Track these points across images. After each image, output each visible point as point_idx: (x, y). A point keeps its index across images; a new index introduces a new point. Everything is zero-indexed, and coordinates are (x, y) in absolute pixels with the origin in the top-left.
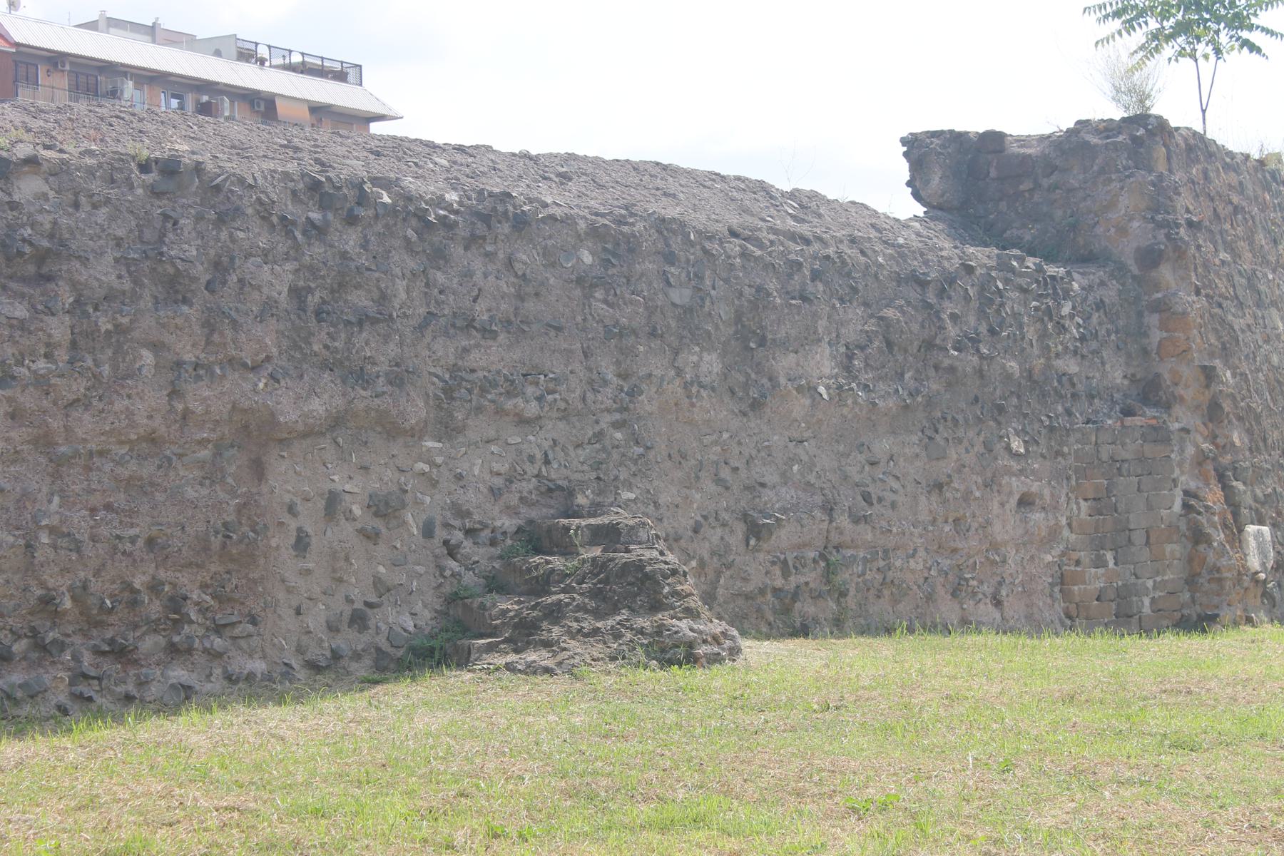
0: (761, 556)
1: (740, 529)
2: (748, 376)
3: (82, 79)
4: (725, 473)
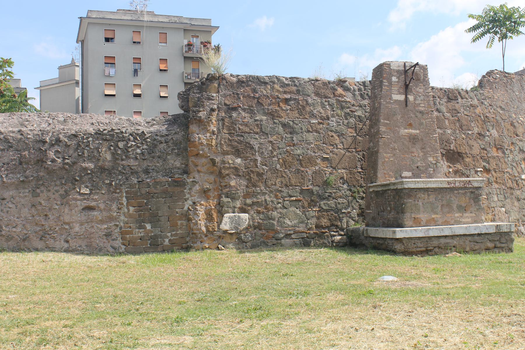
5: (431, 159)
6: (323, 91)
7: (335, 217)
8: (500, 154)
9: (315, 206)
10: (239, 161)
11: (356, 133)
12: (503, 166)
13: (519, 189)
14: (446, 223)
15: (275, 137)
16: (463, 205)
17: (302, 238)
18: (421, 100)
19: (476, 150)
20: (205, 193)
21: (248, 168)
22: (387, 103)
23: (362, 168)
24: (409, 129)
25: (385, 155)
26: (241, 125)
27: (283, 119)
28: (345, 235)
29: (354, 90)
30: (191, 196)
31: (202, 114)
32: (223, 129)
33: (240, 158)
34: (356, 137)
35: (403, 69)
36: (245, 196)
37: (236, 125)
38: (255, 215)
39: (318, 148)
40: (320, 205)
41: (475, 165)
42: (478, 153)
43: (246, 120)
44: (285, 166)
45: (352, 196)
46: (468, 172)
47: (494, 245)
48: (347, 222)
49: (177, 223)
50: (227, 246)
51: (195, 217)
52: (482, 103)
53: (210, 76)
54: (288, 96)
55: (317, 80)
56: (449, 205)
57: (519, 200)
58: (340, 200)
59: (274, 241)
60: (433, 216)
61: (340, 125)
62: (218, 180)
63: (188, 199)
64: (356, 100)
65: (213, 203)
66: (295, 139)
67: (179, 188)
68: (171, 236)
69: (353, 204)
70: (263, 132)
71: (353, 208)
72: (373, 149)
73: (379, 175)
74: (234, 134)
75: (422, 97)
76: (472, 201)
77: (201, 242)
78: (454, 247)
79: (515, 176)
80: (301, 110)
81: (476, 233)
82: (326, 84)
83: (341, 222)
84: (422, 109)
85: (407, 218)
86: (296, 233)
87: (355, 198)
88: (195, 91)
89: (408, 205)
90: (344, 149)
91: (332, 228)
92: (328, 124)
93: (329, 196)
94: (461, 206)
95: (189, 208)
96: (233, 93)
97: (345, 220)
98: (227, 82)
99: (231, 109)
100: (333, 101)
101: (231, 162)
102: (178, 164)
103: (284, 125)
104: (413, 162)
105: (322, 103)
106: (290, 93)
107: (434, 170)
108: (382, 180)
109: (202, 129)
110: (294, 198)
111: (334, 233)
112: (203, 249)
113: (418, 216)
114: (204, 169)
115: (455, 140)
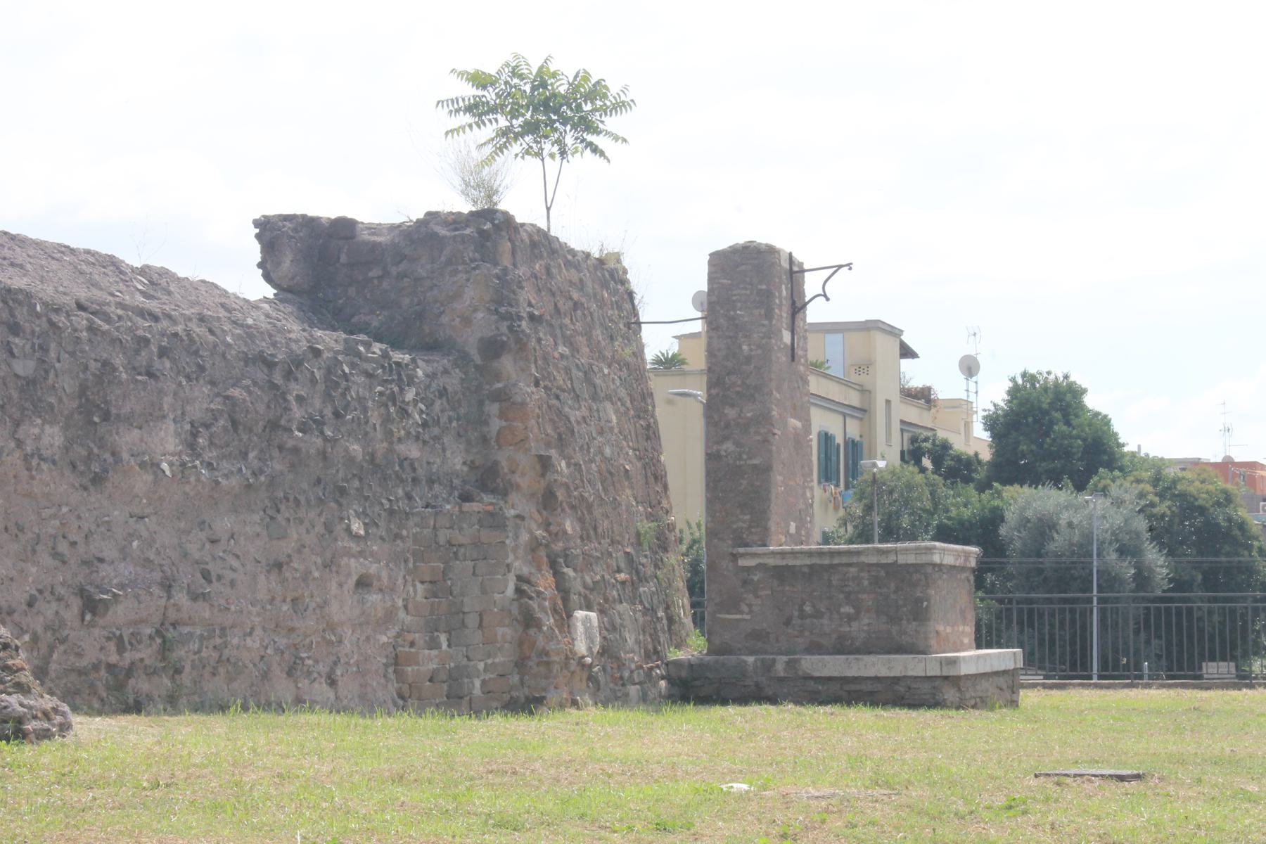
0: (96, 632)
1: (76, 603)
2: (90, 452)
4: (63, 547)
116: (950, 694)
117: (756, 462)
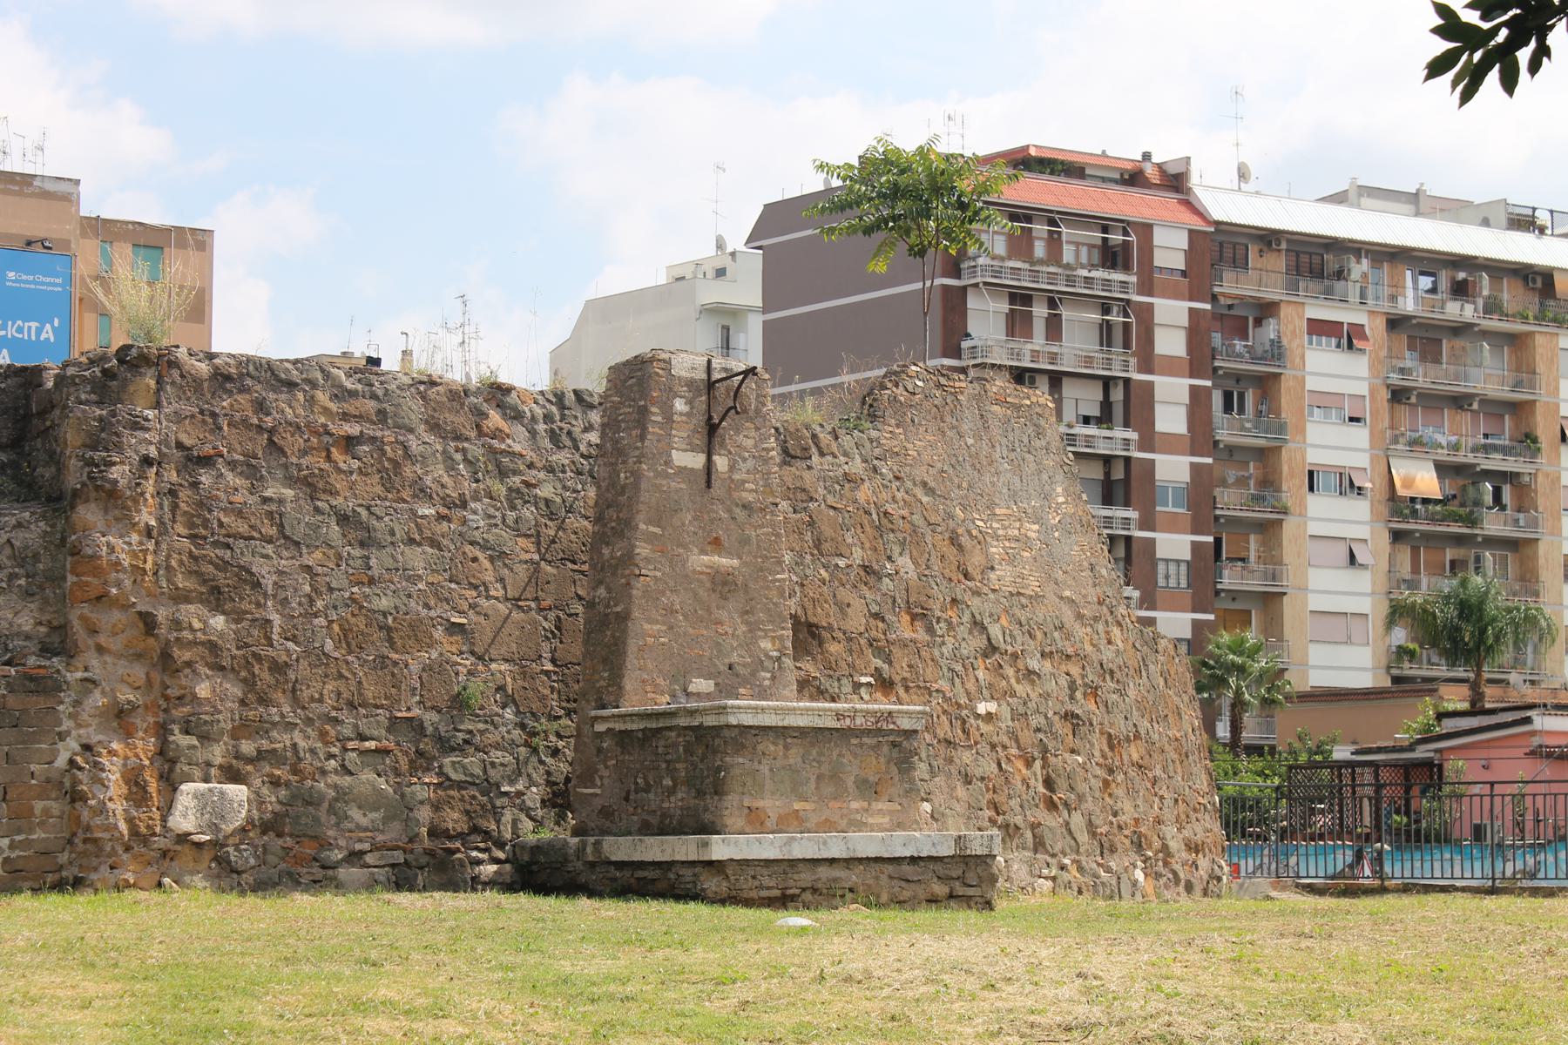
3: (1305, 259)
5: (766, 644)
6: (450, 417)
7: (483, 806)
8: (922, 635)
9: (428, 770)
10: (219, 622)
11: (539, 551)
12: (929, 671)
13: (970, 747)
14: (828, 826)
15: (318, 555)
16: (871, 778)
17: (393, 866)
18: (748, 472)
19: (856, 620)
20: (120, 716)
21: (247, 645)
22: (658, 475)
23: (553, 661)
24: (713, 553)
25: (647, 626)
26: (224, 510)
27: (340, 500)
28: (506, 861)
29: (533, 419)
30: (79, 726)
31: (119, 473)
32: (174, 521)
33: (224, 613)
34: (538, 563)
35: (704, 376)
36: (236, 735)
37: (210, 511)
38: (265, 791)
39: (436, 594)
40: (440, 767)
41: (852, 666)
42: (862, 629)
43: (238, 498)
44: (348, 645)
45: (527, 744)
46: (833, 687)
47: (947, 890)
48: (515, 822)
49: (32, 808)
50: (187, 879)
51: (97, 788)
52: (875, 470)
53: (134, 352)
54: (353, 429)
55: (433, 383)
56: (836, 777)
57: (968, 780)
58: (497, 756)
59: (319, 873)
60: (797, 806)
61: (496, 525)
62: (156, 677)
63: (68, 733)
64: (537, 449)
65: (145, 746)
66: (373, 562)
67: (41, 699)
68: (12, 847)
69: (531, 770)
70: (286, 538)
71: (532, 783)
72: (608, 606)
73: (629, 684)
74: (205, 538)
75: (750, 463)
76: (894, 770)
77: (112, 868)
78: (851, 890)
79: (959, 706)
80: (390, 474)
81: (908, 853)
82: (458, 395)
83: (498, 822)
84: (750, 497)
85: (732, 808)
86: (378, 849)
87: (535, 750)
88: (83, 397)
89: (736, 771)
90: (507, 599)
91: (472, 837)
92: (464, 522)
93: (465, 741)
94: (866, 781)
95: (72, 762)
96: (202, 412)
97: (508, 817)
98: (182, 376)
99: (196, 461)
100: (475, 450)
101: (197, 625)
102: (26, 623)
103: (344, 519)
104: (720, 651)
105: (448, 458)
106: (359, 418)
107: (773, 678)
108: (635, 698)
109: (117, 519)
110: (371, 745)
111: (480, 855)
112: (118, 889)
113: (760, 804)
114: (116, 644)
115: (802, 585)
116: (711, 884)
117: (619, 609)
